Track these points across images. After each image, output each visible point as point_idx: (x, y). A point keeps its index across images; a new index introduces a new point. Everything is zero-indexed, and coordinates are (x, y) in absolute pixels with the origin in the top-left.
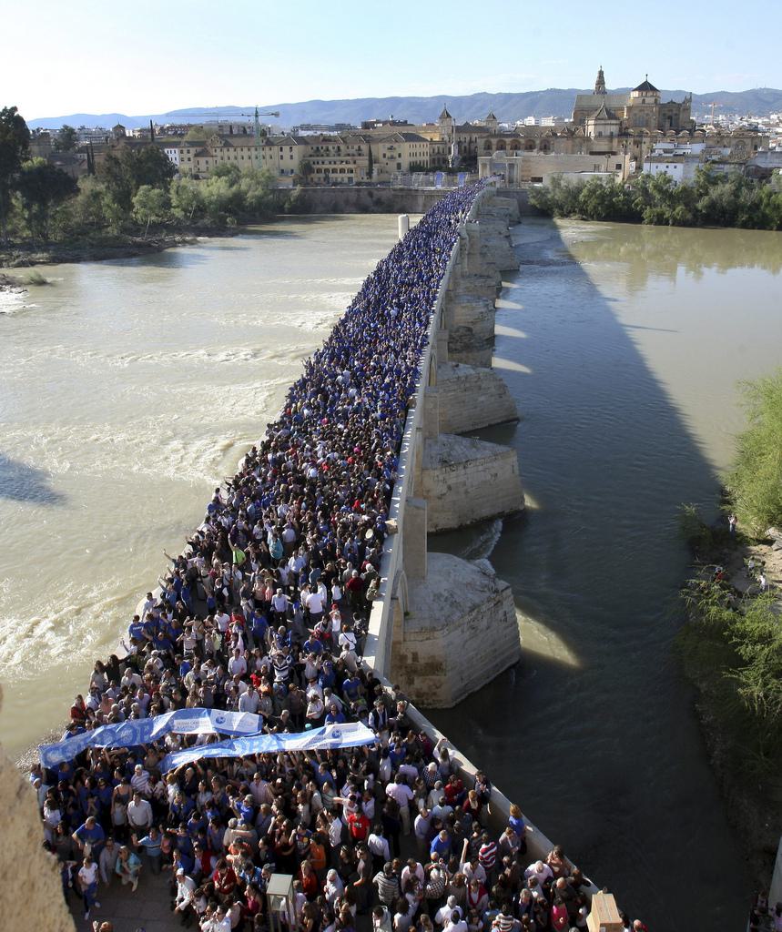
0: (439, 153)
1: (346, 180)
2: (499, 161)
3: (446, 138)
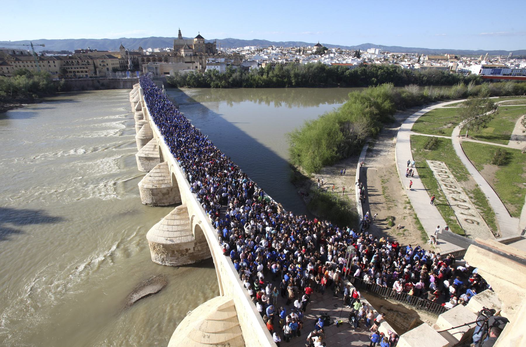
0: (122, 63)
1: (85, 76)
2: (151, 66)
3: (124, 57)
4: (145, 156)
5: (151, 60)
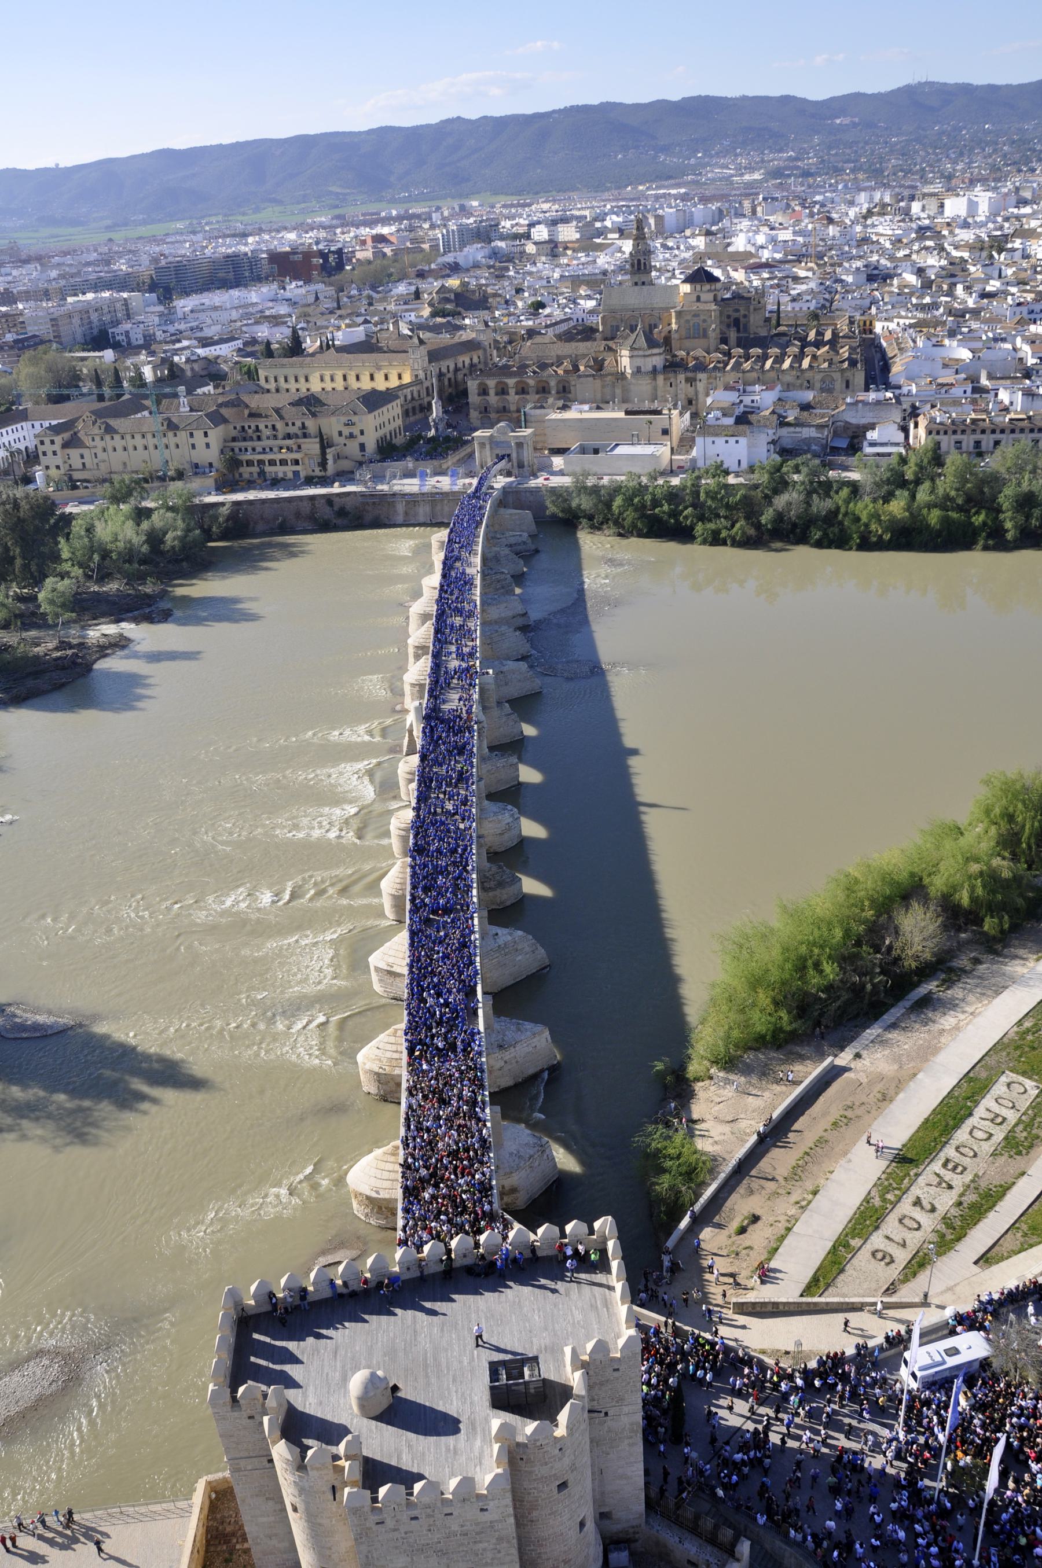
0: (413, 399)
1: (290, 475)
2: (502, 438)
3: (422, 375)
4: (385, 968)
5: (512, 391)
